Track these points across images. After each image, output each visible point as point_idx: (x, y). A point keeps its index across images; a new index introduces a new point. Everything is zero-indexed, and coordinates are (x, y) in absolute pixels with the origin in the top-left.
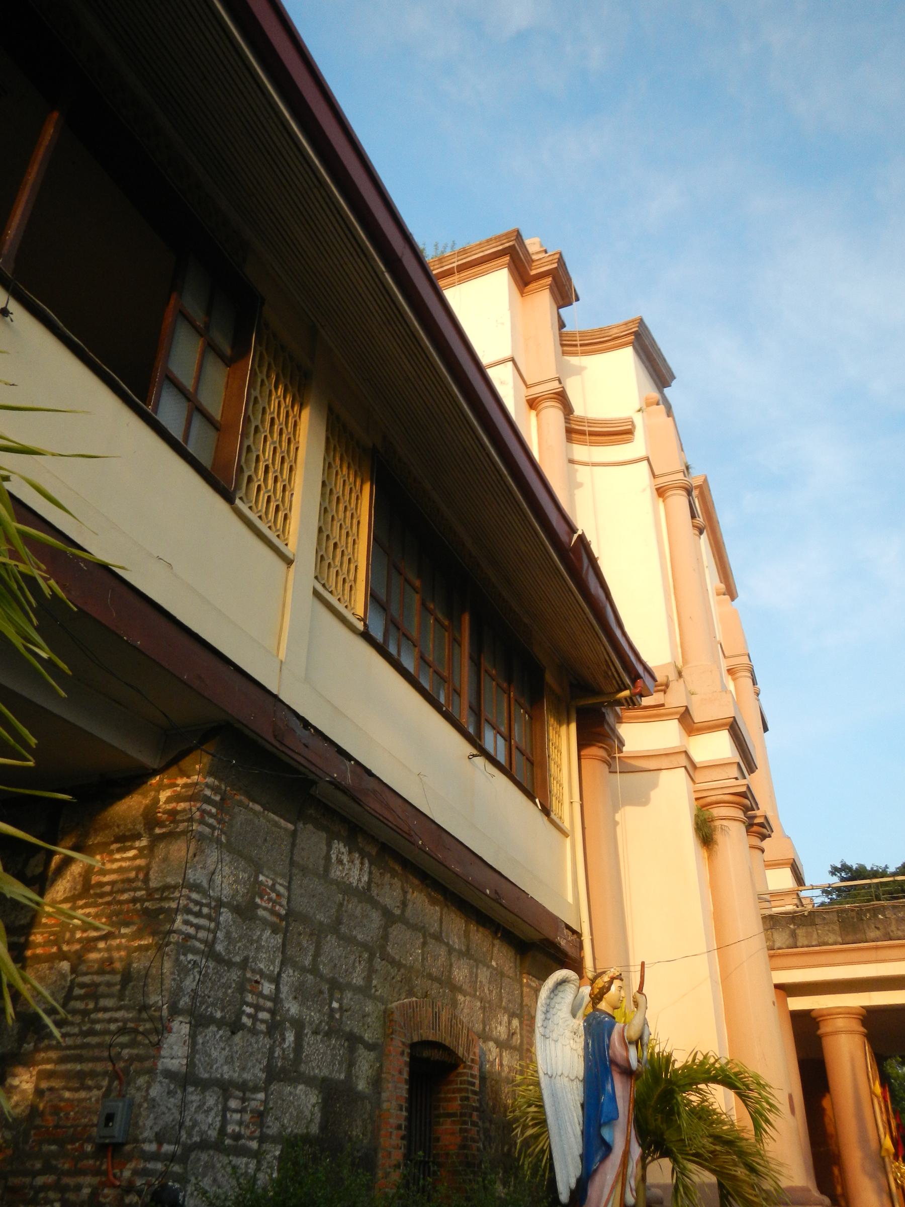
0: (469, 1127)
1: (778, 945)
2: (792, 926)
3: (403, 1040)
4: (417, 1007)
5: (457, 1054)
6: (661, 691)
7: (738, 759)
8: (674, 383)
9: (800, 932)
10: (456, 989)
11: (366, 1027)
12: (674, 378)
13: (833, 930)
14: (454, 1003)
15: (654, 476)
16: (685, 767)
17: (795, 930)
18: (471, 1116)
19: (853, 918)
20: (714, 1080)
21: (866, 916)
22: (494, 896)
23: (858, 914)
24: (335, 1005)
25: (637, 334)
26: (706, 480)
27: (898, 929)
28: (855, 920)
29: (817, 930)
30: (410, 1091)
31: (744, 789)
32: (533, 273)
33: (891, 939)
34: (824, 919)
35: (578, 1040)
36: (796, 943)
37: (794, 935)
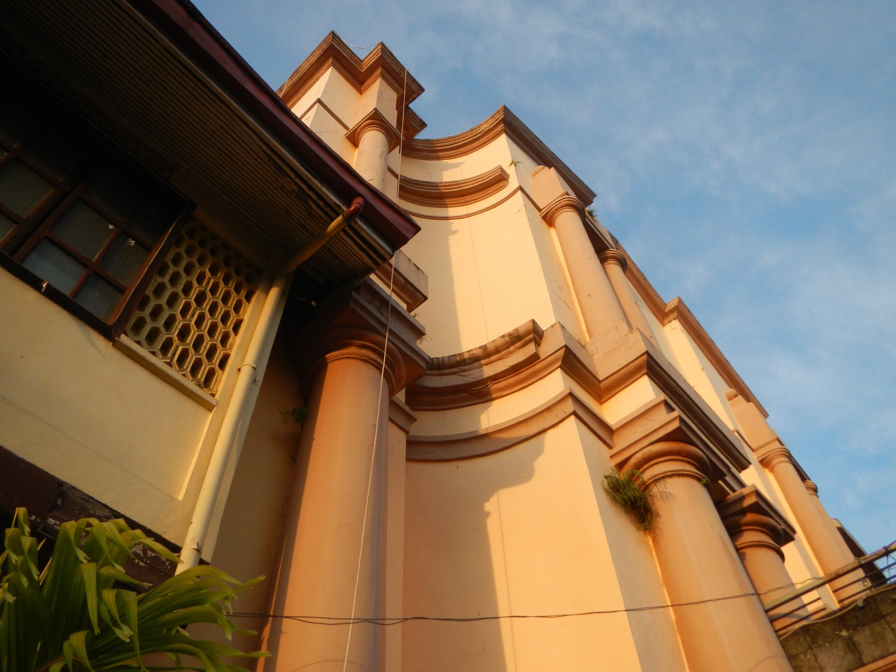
2: (844, 633)
6: (530, 341)
7: (662, 396)
8: (595, 200)
9: (862, 638)
12: (594, 195)
15: (540, 210)
16: (574, 413)
17: (850, 638)
25: (504, 121)
26: (680, 301)
29: (888, 624)
31: (676, 424)
32: (363, 71)
36: (860, 659)
37: (852, 646)
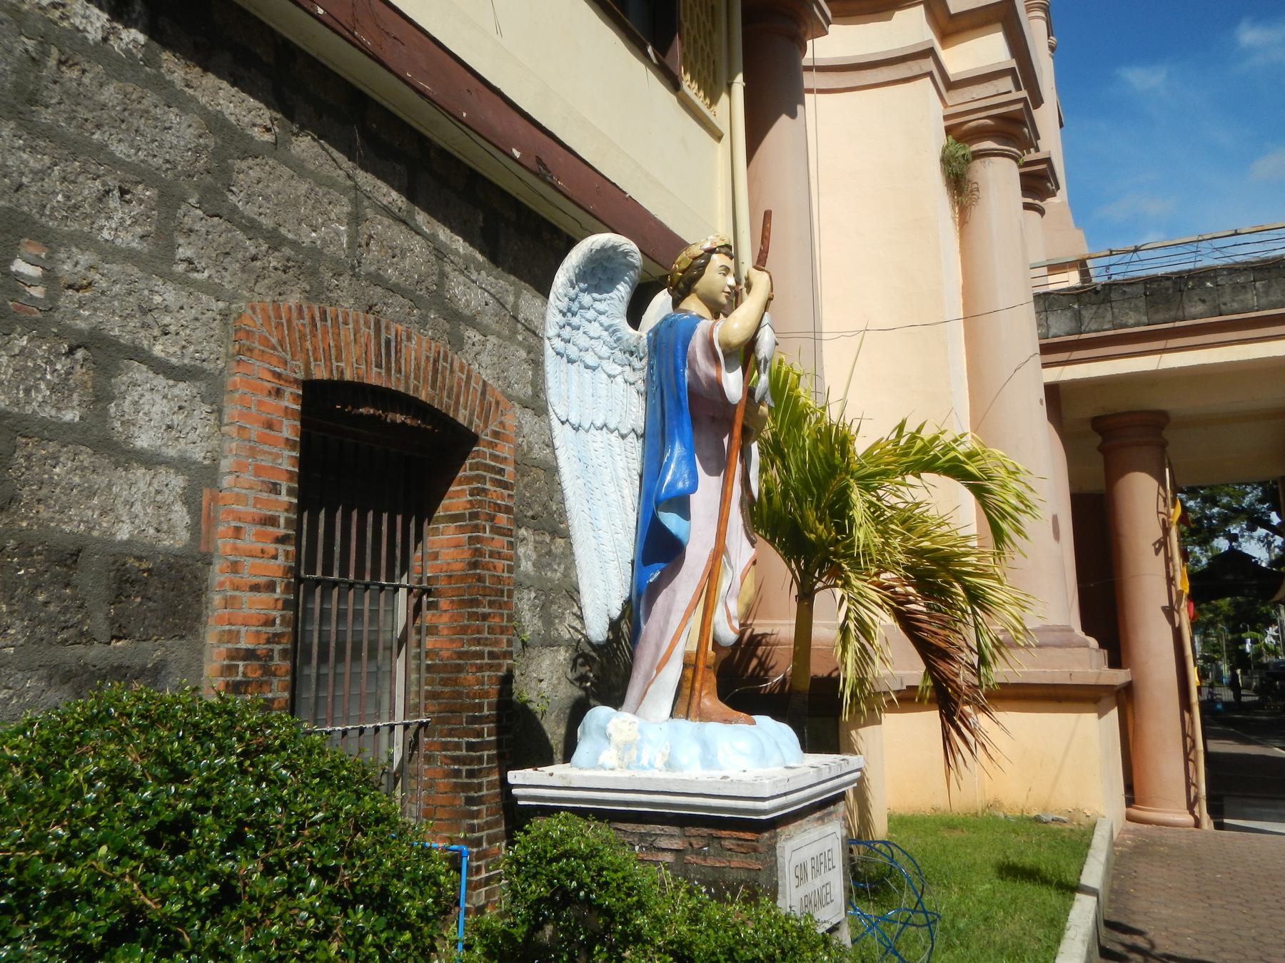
0: (488, 534)
1: (1053, 331)
3: (278, 370)
4: (326, 321)
5: (454, 421)
7: (1013, 64)
9: (1087, 314)
10: (454, 316)
11: (156, 332)
13: (1136, 306)
14: (457, 343)
18: (492, 518)
19: (1167, 289)
20: (929, 465)
21: (1186, 284)
22: (531, 163)
23: (1175, 283)
24: (19, 266)
27: (1233, 301)
28: (1171, 291)
29: (1112, 307)
30: (303, 462)
33: (1221, 315)
34: (1125, 292)
35: (637, 364)
37: (1078, 317)
